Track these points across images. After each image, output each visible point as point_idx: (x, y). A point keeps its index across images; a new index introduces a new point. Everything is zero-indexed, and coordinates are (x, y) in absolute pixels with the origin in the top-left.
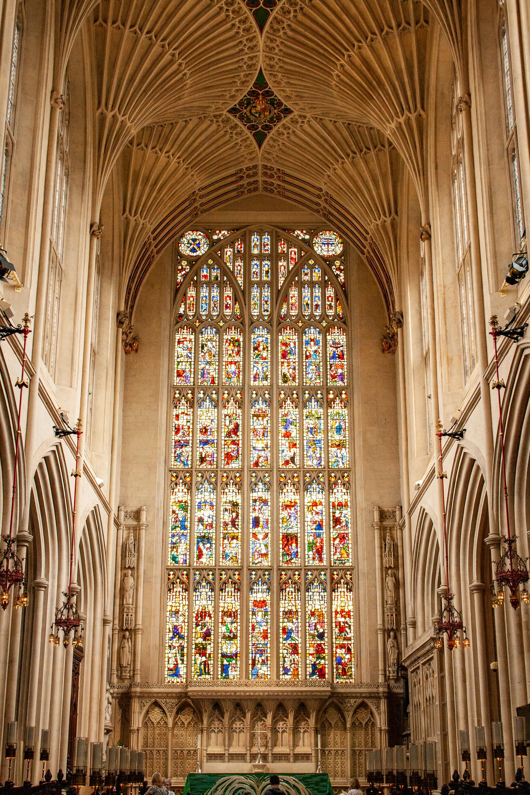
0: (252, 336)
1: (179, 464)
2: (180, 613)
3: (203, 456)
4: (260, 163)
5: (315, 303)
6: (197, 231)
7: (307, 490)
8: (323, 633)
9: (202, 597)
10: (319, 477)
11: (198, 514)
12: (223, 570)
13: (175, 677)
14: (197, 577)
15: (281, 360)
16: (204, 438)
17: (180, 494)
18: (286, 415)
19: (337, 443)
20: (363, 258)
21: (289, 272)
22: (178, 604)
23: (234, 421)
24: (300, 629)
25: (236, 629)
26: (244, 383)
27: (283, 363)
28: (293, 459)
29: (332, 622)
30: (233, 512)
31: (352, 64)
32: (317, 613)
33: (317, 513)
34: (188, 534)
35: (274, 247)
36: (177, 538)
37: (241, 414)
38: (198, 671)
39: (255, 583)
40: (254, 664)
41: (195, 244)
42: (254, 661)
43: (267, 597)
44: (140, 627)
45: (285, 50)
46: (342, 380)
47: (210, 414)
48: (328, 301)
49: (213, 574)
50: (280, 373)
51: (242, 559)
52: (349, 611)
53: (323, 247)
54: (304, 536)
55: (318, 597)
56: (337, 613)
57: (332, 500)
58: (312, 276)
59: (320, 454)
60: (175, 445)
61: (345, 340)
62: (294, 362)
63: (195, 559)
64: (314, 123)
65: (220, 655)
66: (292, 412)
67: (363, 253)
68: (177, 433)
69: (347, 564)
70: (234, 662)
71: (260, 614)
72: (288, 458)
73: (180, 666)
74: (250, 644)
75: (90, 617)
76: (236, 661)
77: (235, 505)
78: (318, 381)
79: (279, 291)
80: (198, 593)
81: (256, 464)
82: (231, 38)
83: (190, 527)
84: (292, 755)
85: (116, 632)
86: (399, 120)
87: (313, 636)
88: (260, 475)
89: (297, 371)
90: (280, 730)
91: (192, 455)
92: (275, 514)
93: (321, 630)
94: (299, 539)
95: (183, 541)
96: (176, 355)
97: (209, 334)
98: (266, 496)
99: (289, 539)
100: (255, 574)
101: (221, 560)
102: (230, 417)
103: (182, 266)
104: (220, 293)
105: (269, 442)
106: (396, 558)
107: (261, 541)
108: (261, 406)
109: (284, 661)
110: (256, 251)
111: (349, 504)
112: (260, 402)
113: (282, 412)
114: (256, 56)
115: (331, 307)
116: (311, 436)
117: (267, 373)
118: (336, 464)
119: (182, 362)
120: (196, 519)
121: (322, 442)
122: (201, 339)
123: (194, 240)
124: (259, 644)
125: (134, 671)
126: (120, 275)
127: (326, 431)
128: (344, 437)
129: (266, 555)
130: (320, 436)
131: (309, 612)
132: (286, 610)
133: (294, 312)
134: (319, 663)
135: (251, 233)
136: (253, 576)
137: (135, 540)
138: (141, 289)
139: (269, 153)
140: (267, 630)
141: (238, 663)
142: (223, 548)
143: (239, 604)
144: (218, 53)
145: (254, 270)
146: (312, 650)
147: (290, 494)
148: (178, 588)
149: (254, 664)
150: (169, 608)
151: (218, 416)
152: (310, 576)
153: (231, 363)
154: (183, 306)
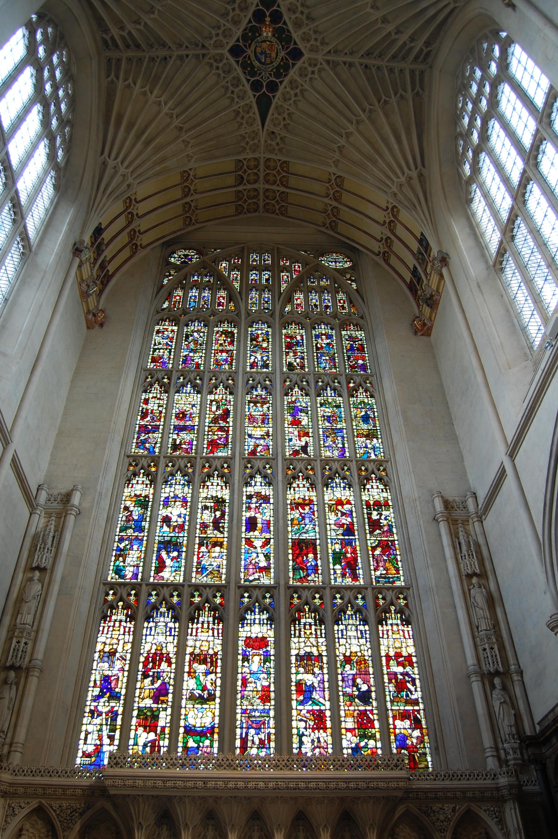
1: (142, 451)
2: (118, 655)
3: (178, 442)
6: (190, 249)
7: (327, 485)
8: (369, 691)
9: (158, 630)
11: (163, 512)
16: (182, 423)
18: (294, 402)
19: (365, 433)
22: (115, 641)
23: (224, 407)
25: (214, 683)
28: (304, 449)
29: (383, 674)
30: (215, 511)
32: (355, 659)
33: (343, 514)
34: (145, 538)
36: (127, 542)
37: (232, 400)
39: (250, 609)
42: (244, 741)
48: (340, 303)
50: (284, 362)
51: (228, 573)
52: (410, 656)
54: (327, 543)
55: (355, 633)
56: (388, 657)
57: (364, 498)
58: (319, 283)
59: (343, 444)
60: (139, 431)
62: (302, 353)
63: (152, 573)
65: (182, 730)
66: (301, 400)
68: (143, 418)
69: (398, 584)
70: (207, 743)
71: (256, 659)
76: (212, 741)
77: (219, 502)
80: (152, 624)
81: (254, 452)
83: (149, 529)
87: (351, 697)
88: (259, 464)
89: (306, 361)
91: (161, 443)
93: (364, 688)
94: (318, 547)
95: (135, 547)
96: (153, 342)
101: (194, 575)
102: (217, 403)
103: (170, 273)
105: (271, 430)
107: (259, 550)
109: (301, 743)
111: (390, 504)
116: (327, 424)
118: (366, 456)
119: (159, 349)
120: (160, 517)
121: (345, 431)
123: (186, 256)
124: (255, 710)
128: (375, 426)
129: (266, 569)
131: (342, 658)
132: (302, 653)
134: (366, 746)
140: (269, 686)
142: (198, 558)
143: (220, 642)
146: (350, 723)
149: (244, 747)
151: (201, 402)
152: (339, 601)
153: (222, 351)
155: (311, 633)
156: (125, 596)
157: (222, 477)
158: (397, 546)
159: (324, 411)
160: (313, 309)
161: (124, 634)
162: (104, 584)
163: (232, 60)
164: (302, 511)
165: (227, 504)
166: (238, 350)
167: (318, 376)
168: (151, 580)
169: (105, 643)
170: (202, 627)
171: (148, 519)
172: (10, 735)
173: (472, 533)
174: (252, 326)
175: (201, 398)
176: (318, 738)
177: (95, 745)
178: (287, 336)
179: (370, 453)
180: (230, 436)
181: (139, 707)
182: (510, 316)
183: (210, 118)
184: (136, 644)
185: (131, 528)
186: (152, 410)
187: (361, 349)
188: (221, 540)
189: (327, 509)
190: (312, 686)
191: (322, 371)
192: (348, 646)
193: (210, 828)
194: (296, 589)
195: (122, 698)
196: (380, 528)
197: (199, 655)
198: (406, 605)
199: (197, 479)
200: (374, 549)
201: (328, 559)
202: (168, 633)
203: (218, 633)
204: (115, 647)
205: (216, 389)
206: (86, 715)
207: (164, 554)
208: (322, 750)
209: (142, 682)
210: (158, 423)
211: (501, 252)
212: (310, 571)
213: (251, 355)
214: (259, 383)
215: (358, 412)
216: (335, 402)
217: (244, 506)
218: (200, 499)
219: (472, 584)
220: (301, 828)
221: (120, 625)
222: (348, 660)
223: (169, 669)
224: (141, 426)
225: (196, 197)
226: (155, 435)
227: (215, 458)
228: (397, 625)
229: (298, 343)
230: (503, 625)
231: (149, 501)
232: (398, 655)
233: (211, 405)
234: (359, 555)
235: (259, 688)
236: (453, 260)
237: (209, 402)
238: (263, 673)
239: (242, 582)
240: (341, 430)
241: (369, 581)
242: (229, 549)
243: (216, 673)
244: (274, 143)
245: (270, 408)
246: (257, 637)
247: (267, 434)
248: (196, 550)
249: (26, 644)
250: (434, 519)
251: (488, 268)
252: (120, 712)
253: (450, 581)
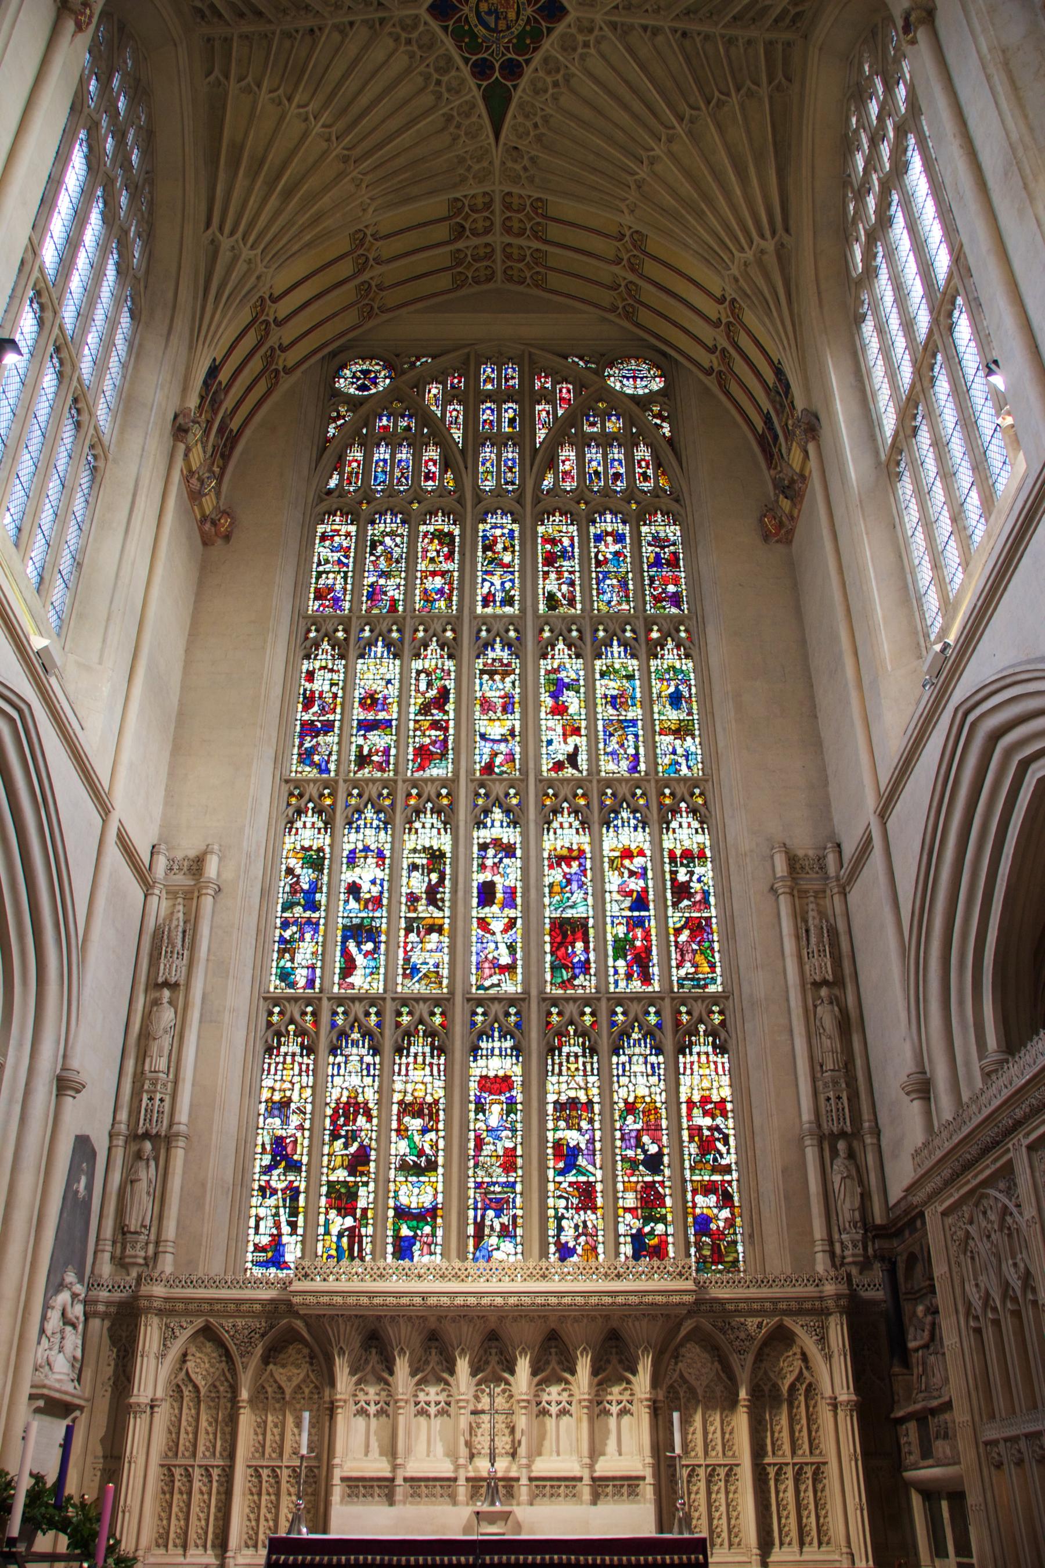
0: (481, 527)
1: (308, 769)
2: (293, 1106)
3: (365, 752)
5: (611, 472)
6: (372, 359)
7: (608, 824)
8: (660, 1155)
9: (350, 1067)
10: (634, 795)
11: (349, 876)
13: (273, 1270)
14: (340, 1020)
16: (370, 716)
17: (308, 833)
22: (288, 1085)
23: (438, 684)
24: (598, 1145)
25: (434, 1145)
26: (460, 609)
27: (546, 573)
28: (572, 759)
29: (681, 1129)
30: (430, 872)
33: (632, 874)
36: (294, 929)
37: (453, 669)
38: (333, 1252)
39: (485, 1033)
40: (479, 1236)
41: (368, 378)
42: (479, 1227)
43: (515, 1070)
44: (182, 1128)
46: (678, 607)
47: (383, 670)
48: (640, 467)
49: (377, 1014)
50: (540, 591)
52: (723, 1101)
53: (625, 381)
54: (605, 924)
55: (642, 1068)
56: (690, 1103)
57: (667, 844)
58: (603, 426)
59: (636, 748)
61: (678, 533)
62: (571, 573)
63: (336, 979)
65: (391, 1213)
66: (568, 666)
68: (307, 707)
69: (712, 989)
70: (427, 1229)
71: (496, 1109)
73: (285, 1239)
74: (472, 1185)
75: (16, 1068)
77: (435, 856)
81: (489, 768)
83: (327, 906)
84: (587, 1481)
85: (120, 1141)
87: (633, 1164)
88: (498, 790)
89: (578, 588)
90: (554, 1409)
91: (339, 752)
93: (653, 1149)
94: (591, 931)
95: (308, 936)
96: (316, 560)
98: (510, 835)
100: (484, 1014)
101: (400, 979)
102: (428, 674)
103: (338, 412)
104: (413, 455)
105: (517, 724)
107: (499, 937)
108: (499, 652)
109: (560, 1229)
111: (708, 854)
113: (545, 665)
115: (645, 477)
116: (611, 711)
117: (512, 593)
118: (673, 769)
119: (328, 573)
120: (343, 885)
121: (640, 723)
122: (370, 532)
124: (494, 1184)
125: (157, 1243)
126: (190, 348)
127: (648, 703)
128: (690, 714)
129: (510, 968)
131: (622, 1105)
132: (563, 1098)
136: (479, 1018)
140: (515, 1149)
141: (439, 1232)
142: (406, 952)
143: (442, 1084)
145: (485, 417)
146: (630, 1200)
147: (566, 831)
149: (479, 1236)
150: (266, 1094)
151: (401, 674)
152: (621, 1018)
153: (434, 574)
154: (336, 477)
155: (577, 1069)
156: (297, 1017)
157: (439, 813)
158: (714, 927)
159: (606, 686)
160: (591, 481)
161: (300, 1075)
162: (265, 999)
163: (435, 25)
164: (567, 870)
165: (448, 861)
166: (461, 570)
167: (598, 621)
168: (336, 989)
169: (273, 1089)
170: (415, 1062)
171: (325, 889)
172: (154, 1230)
173: (830, 912)
174: (484, 521)
175: (401, 666)
176: (585, 1222)
177: (271, 1235)
178: (547, 540)
179: (680, 764)
180: (451, 738)
181: (328, 1181)
182: (903, 568)
183: (399, 132)
185: (299, 904)
186: (321, 693)
187: (673, 562)
188: (440, 922)
189: (606, 866)
190: (577, 1148)
191: (604, 608)
192: (631, 1088)
193: (434, 1351)
194: (555, 1001)
195: (304, 1168)
196: (690, 896)
197: (411, 1104)
198: (723, 1023)
199: (399, 818)
200: (678, 931)
201: (606, 950)
202: (365, 1072)
203: (439, 1071)
204: (288, 1094)
205: (425, 650)
206: (255, 1193)
207: (352, 946)
208: (589, 1238)
209: (331, 1144)
210: (331, 717)
211: (896, 448)
212: (577, 971)
213: (484, 580)
214: (498, 635)
215: (664, 687)
216: (626, 668)
217: (475, 863)
218: (406, 852)
219: (820, 997)
220: (553, 1350)
221: (293, 1061)
222: (630, 1108)
223: (368, 1126)
224: (304, 724)
225: (379, 270)
226: (329, 739)
227: (426, 781)
228: (707, 1054)
229: (564, 555)
230: (859, 1062)
231: (324, 858)
233: (417, 680)
234: (654, 942)
235: (501, 1152)
236: (825, 432)
237: (414, 675)
238: (506, 1128)
239: (474, 990)
240: (634, 722)
241: (667, 987)
242: (452, 937)
243: (437, 1131)
244: (518, 167)
245: (517, 683)
246: (496, 1076)
248: (402, 939)
249: (162, 1100)
250: (772, 888)
251: (878, 464)
252: (302, 1188)
253: (787, 992)
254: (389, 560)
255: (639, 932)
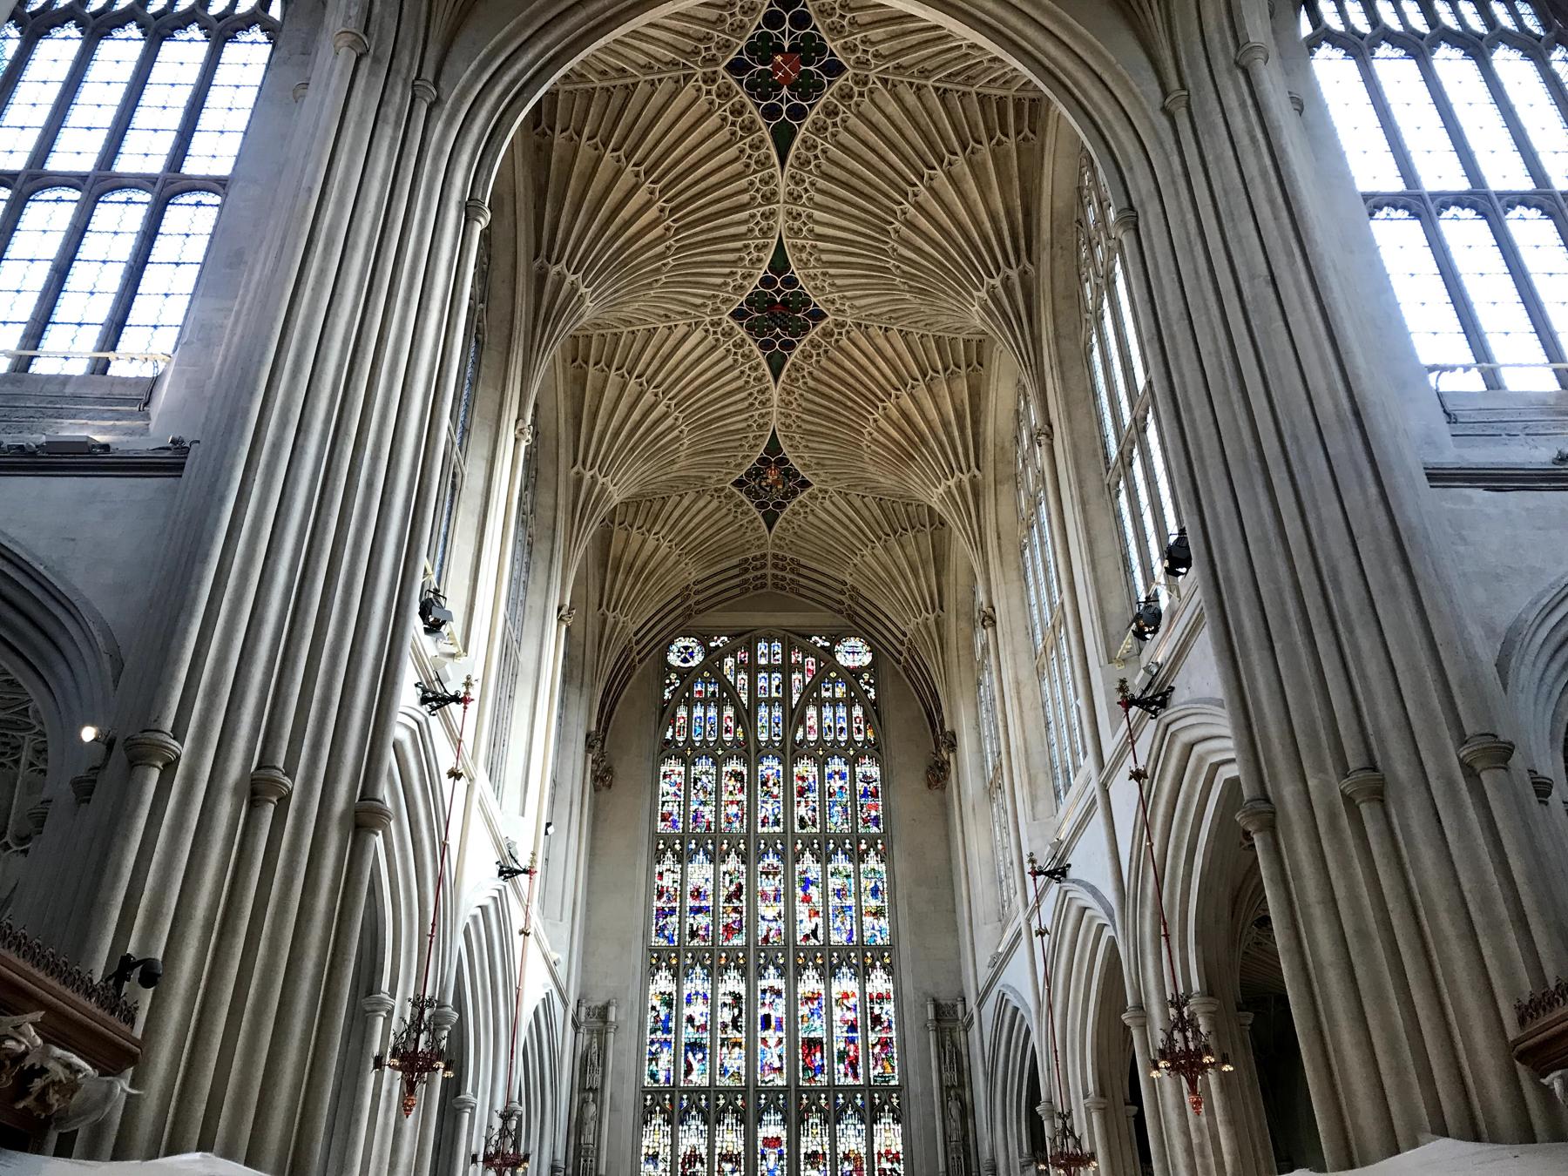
0: (760, 768)
4: (770, 551)
5: (838, 726)
12: (721, 1092)
15: (796, 799)
18: (805, 872)
20: (899, 668)
21: (805, 687)
23: (736, 881)
27: (799, 802)
28: (814, 933)
31: (888, 417)
32: (852, 1156)
33: (849, 1009)
35: (786, 655)
36: (657, 1045)
39: (766, 1110)
41: (687, 653)
45: (804, 404)
51: (747, 1075)
57: (869, 990)
58: (834, 692)
64: (837, 498)
67: (898, 662)
68: (660, 896)
69: (892, 1083)
72: (809, 932)
77: (737, 997)
78: (846, 826)
79: (793, 711)
80: (686, 1128)
81: (766, 939)
82: (739, 389)
86: (948, 483)
92: (791, 1009)
95: (665, 1050)
97: (704, 765)
98: (779, 984)
99: (812, 1044)
106: (960, 1072)
108: (772, 860)
110: (763, 661)
112: (771, 855)
113: (799, 868)
114: (768, 413)
123: (686, 648)
127: (858, 895)
129: (780, 1069)
130: (851, 901)
132: (809, 1151)
133: (812, 737)
135: (758, 640)
137: (599, 1048)
138: (617, 707)
139: (781, 539)
144: (723, 407)
148: (658, 1120)
152: (841, 1101)
153: (732, 802)
154: (671, 730)
184: (674, 1146)
207: (690, 1054)
210: (674, 904)
222: (846, 1157)
232: (888, 1152)
240: (850, 907)
247: (779, 914)
254: (705, 792)
255: (852, 1047)
